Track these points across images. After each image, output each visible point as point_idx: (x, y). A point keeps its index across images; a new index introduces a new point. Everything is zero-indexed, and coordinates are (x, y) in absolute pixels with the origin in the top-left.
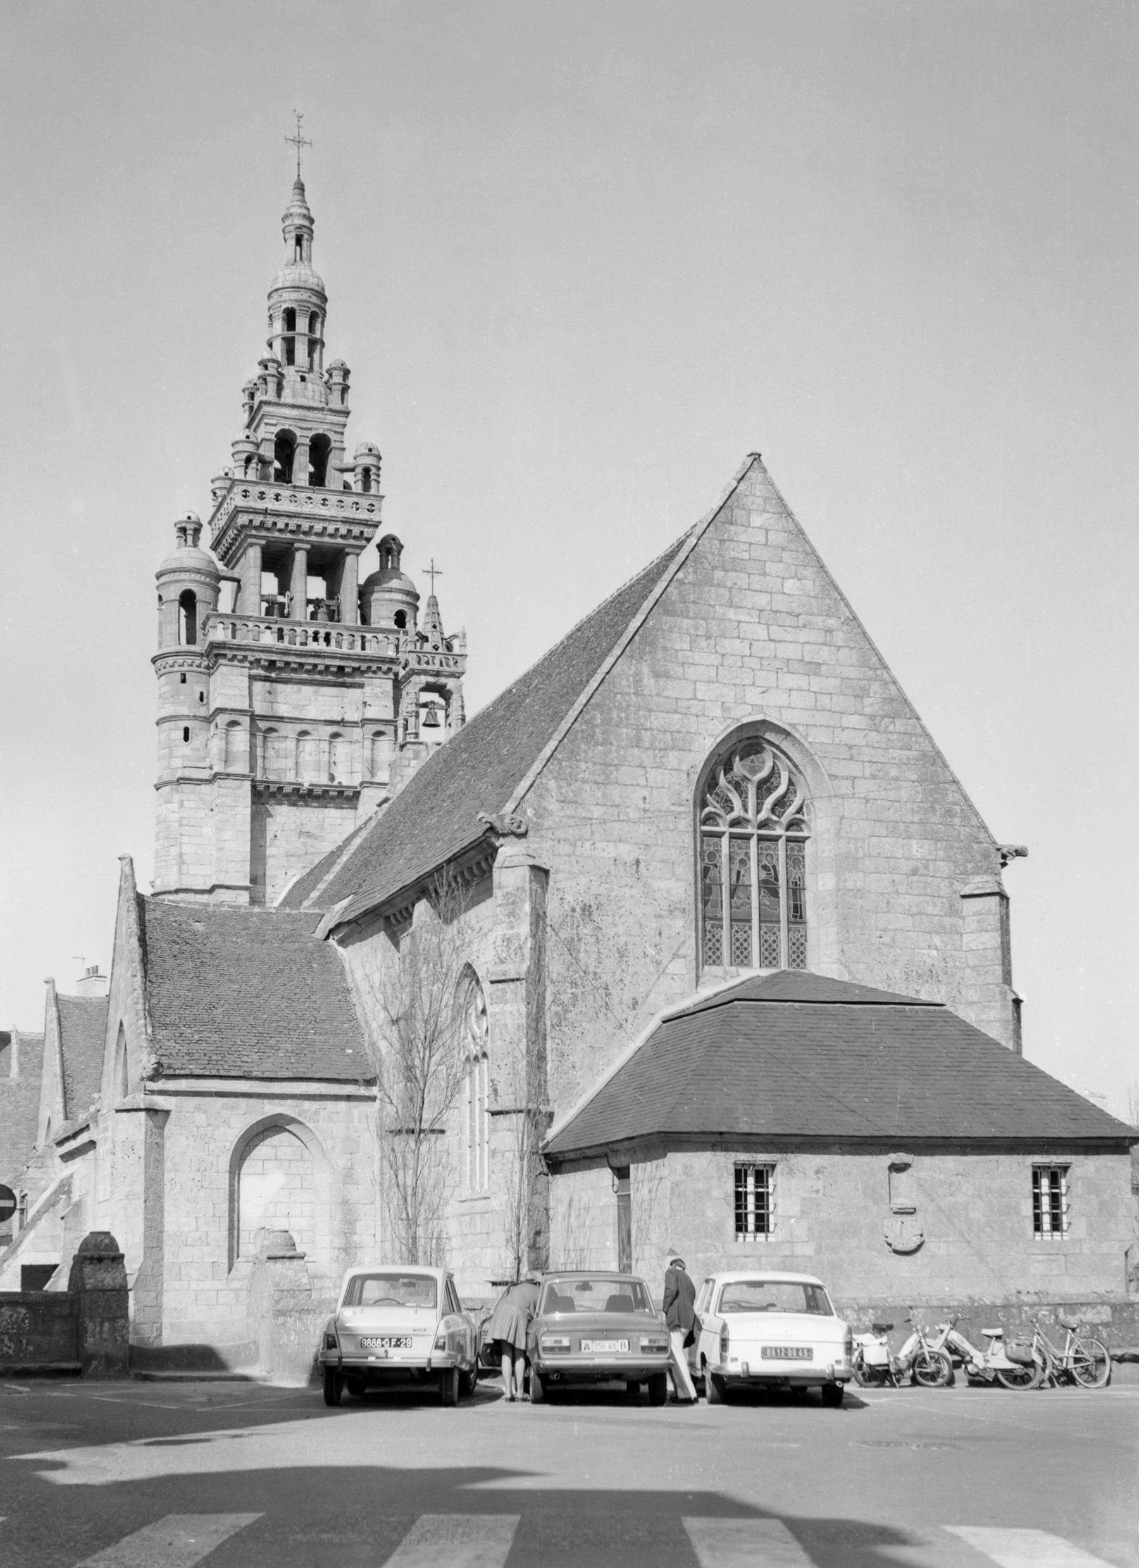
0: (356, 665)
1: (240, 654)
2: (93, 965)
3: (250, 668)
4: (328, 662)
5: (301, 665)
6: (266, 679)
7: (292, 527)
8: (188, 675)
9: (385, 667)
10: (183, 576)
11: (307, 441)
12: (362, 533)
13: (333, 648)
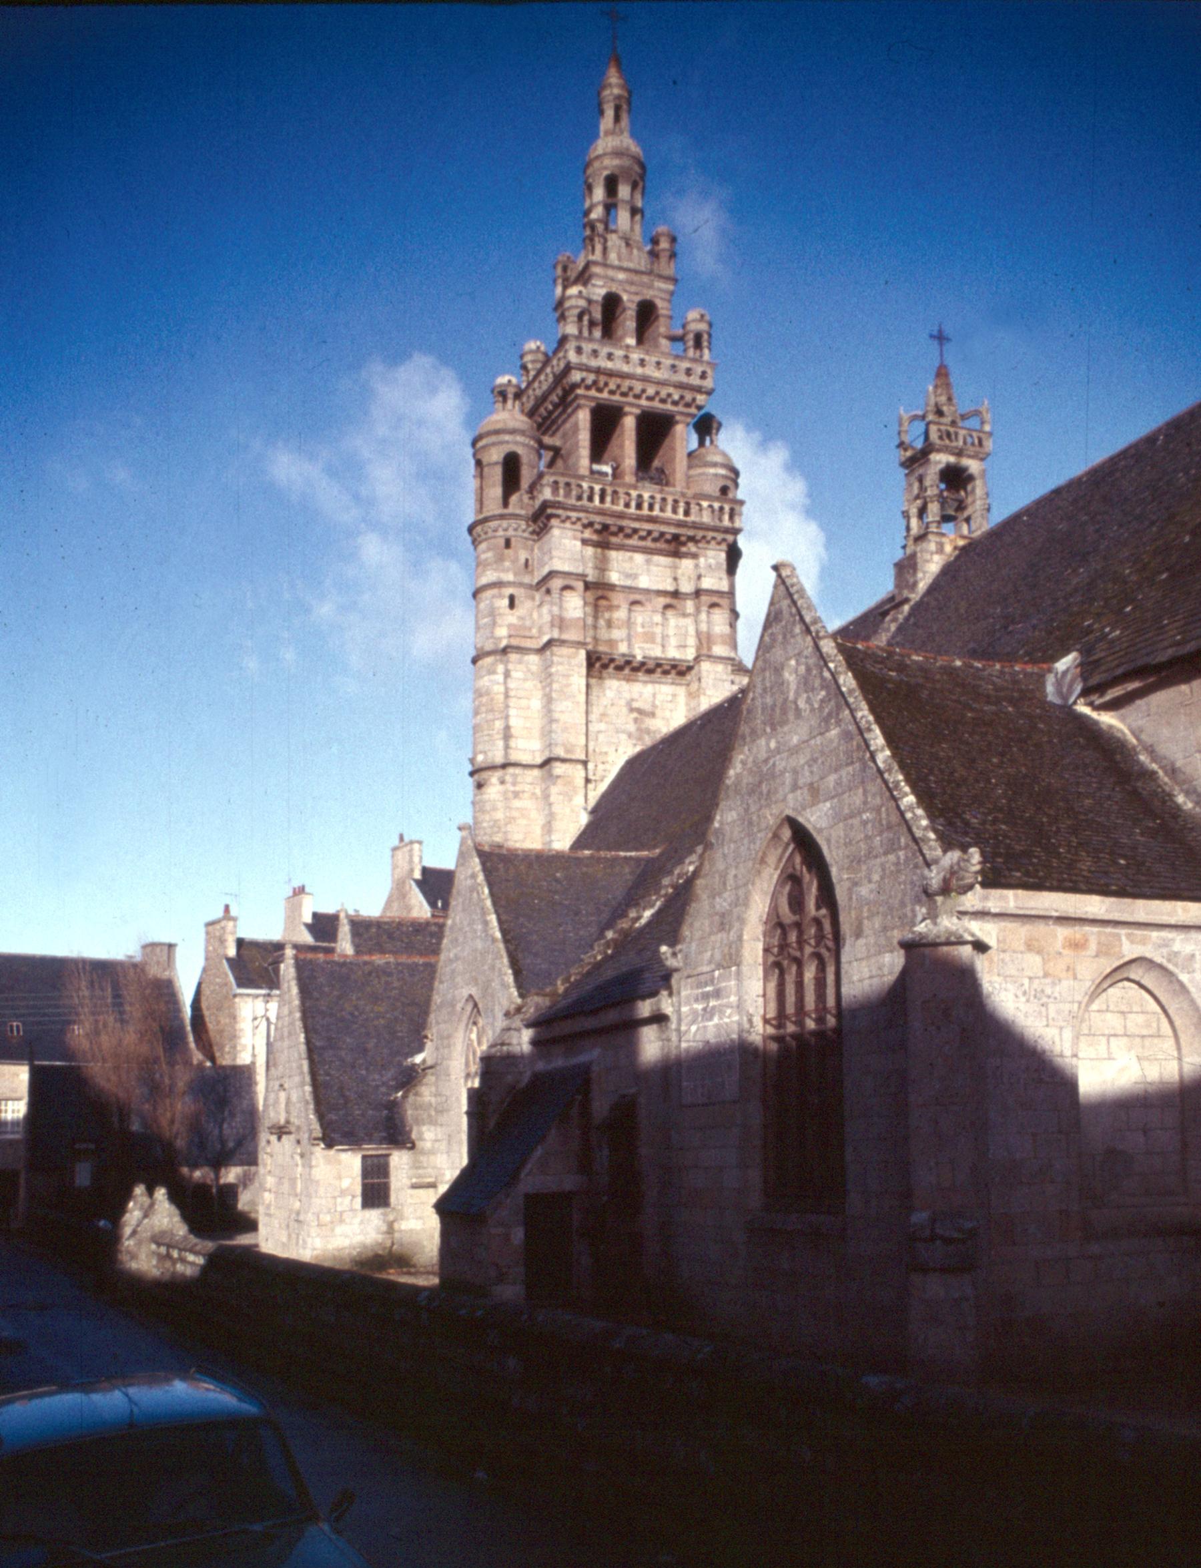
0: (691, 533)
1: (574, 515)
2: (300, 884)
3: (582, 532)
4: (663, 528)
5: (635, 531)
6: (596, 545)
7: (624, 389)
8: (513, 541)
9: (720, 536)
10: (507, 437)
11: (634, 306)
12: (694, 400)
13: (668, 514)
